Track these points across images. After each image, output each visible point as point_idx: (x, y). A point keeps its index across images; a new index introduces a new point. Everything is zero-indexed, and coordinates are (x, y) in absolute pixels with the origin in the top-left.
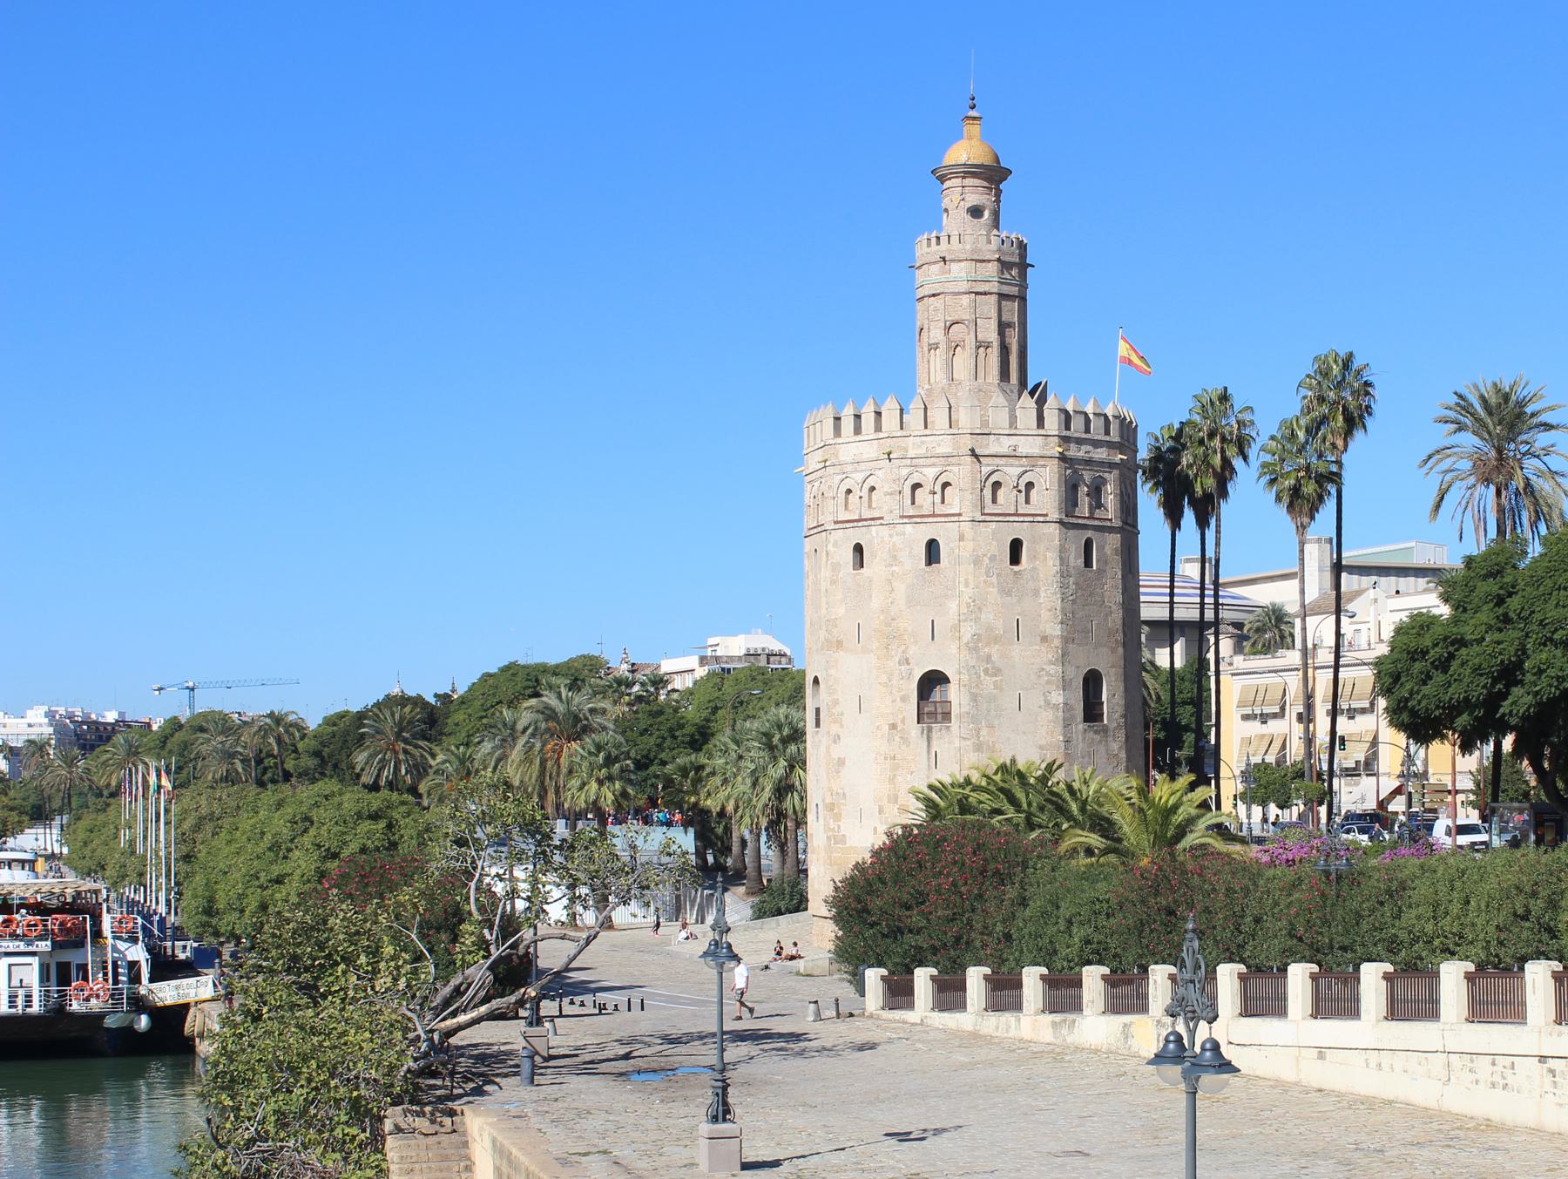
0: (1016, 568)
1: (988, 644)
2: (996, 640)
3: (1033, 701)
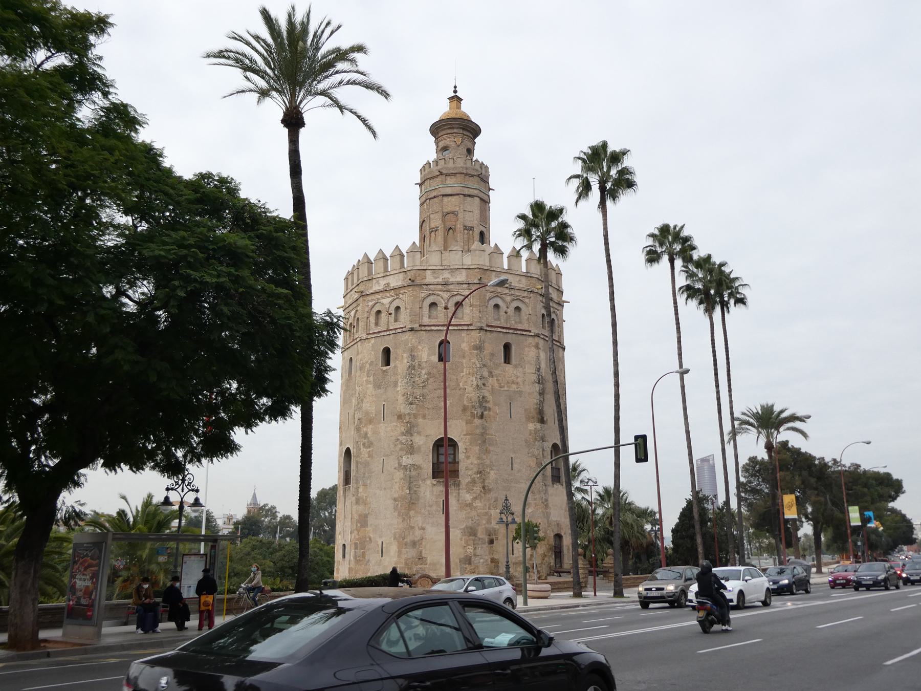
0: (385, 368)
1: (366, 425)
2: (371, 421)
3: (392, 463)
